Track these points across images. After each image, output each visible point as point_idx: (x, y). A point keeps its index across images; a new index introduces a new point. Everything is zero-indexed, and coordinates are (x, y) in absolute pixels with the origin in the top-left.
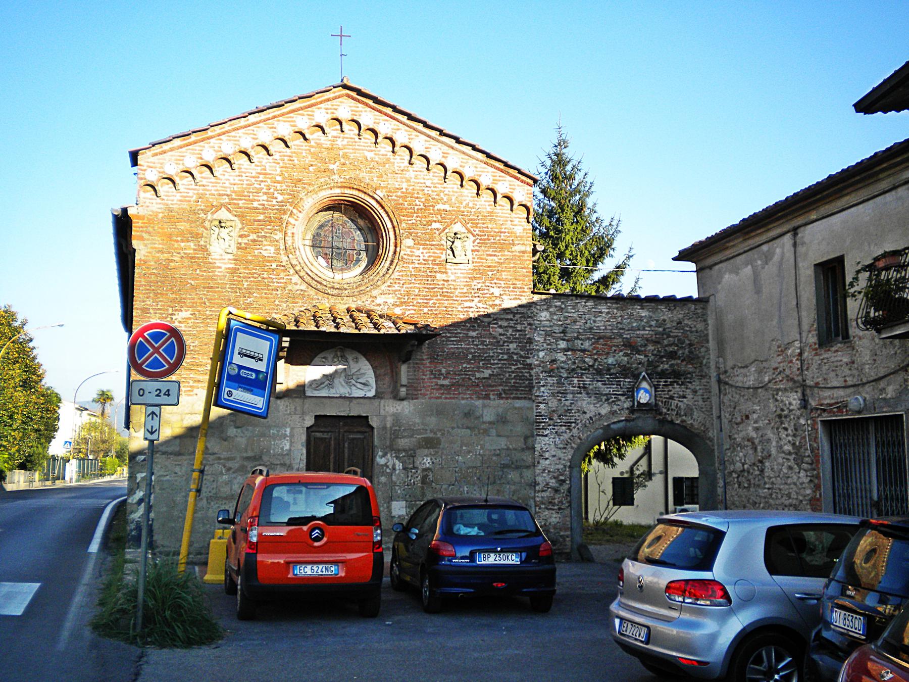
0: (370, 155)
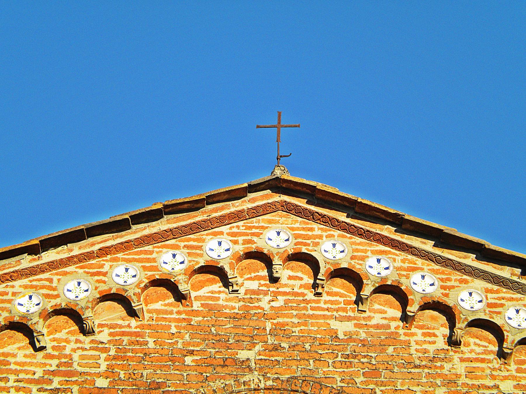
0: (343, 328)
